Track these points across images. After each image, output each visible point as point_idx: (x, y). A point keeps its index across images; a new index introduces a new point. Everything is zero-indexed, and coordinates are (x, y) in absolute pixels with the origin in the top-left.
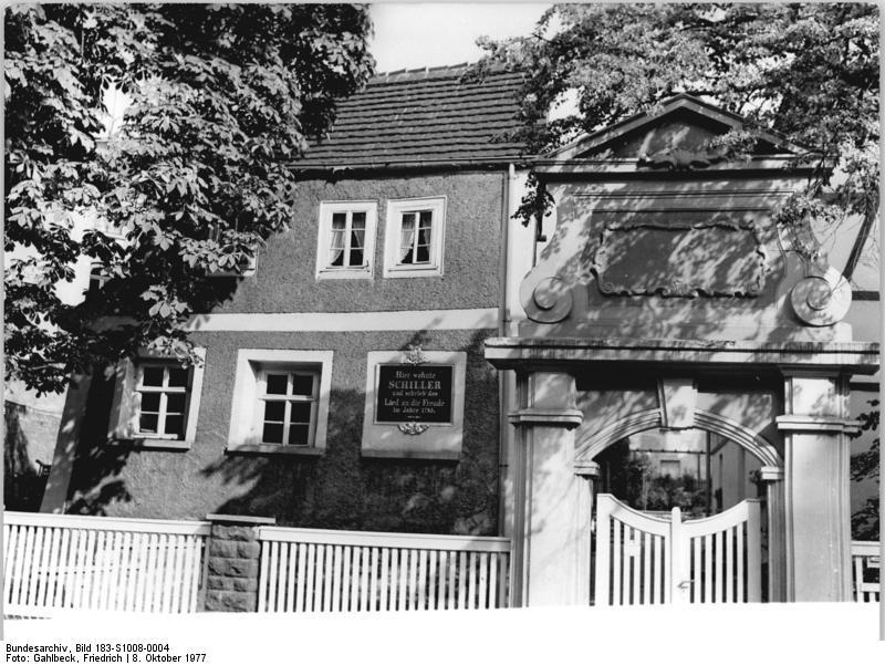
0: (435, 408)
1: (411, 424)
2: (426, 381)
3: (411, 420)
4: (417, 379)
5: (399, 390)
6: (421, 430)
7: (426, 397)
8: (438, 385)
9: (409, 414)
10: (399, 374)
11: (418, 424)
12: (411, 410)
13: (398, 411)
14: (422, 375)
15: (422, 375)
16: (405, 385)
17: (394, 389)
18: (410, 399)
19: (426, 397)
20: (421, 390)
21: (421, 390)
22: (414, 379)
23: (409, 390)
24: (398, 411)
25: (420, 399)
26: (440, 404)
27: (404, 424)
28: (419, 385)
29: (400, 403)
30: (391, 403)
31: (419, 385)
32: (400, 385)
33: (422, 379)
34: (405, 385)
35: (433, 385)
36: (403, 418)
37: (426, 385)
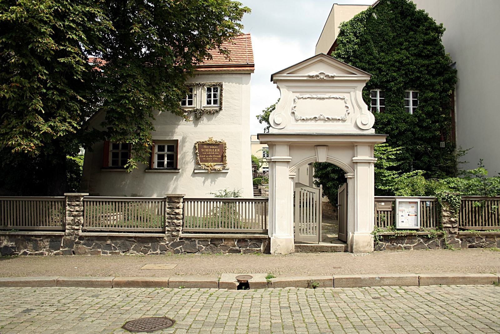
1: (210, 164)
3: (209, 162)
4: (212, 148)
6: (213, 165)
8: (218, 150)
10: (205, 147)
11: (212, 163)
12: (209, 159)
13: (205, 159)
15: (213, 147)
16: (207, 150)
18: (209, 155)
24: (205, 159)
25: (212, 155)
27: (207, 163)
28: (212, 150)
29: (205, 156)
31: (212, 150)
35: (217, 150)
36: (207, 161)
37: (214, 150)
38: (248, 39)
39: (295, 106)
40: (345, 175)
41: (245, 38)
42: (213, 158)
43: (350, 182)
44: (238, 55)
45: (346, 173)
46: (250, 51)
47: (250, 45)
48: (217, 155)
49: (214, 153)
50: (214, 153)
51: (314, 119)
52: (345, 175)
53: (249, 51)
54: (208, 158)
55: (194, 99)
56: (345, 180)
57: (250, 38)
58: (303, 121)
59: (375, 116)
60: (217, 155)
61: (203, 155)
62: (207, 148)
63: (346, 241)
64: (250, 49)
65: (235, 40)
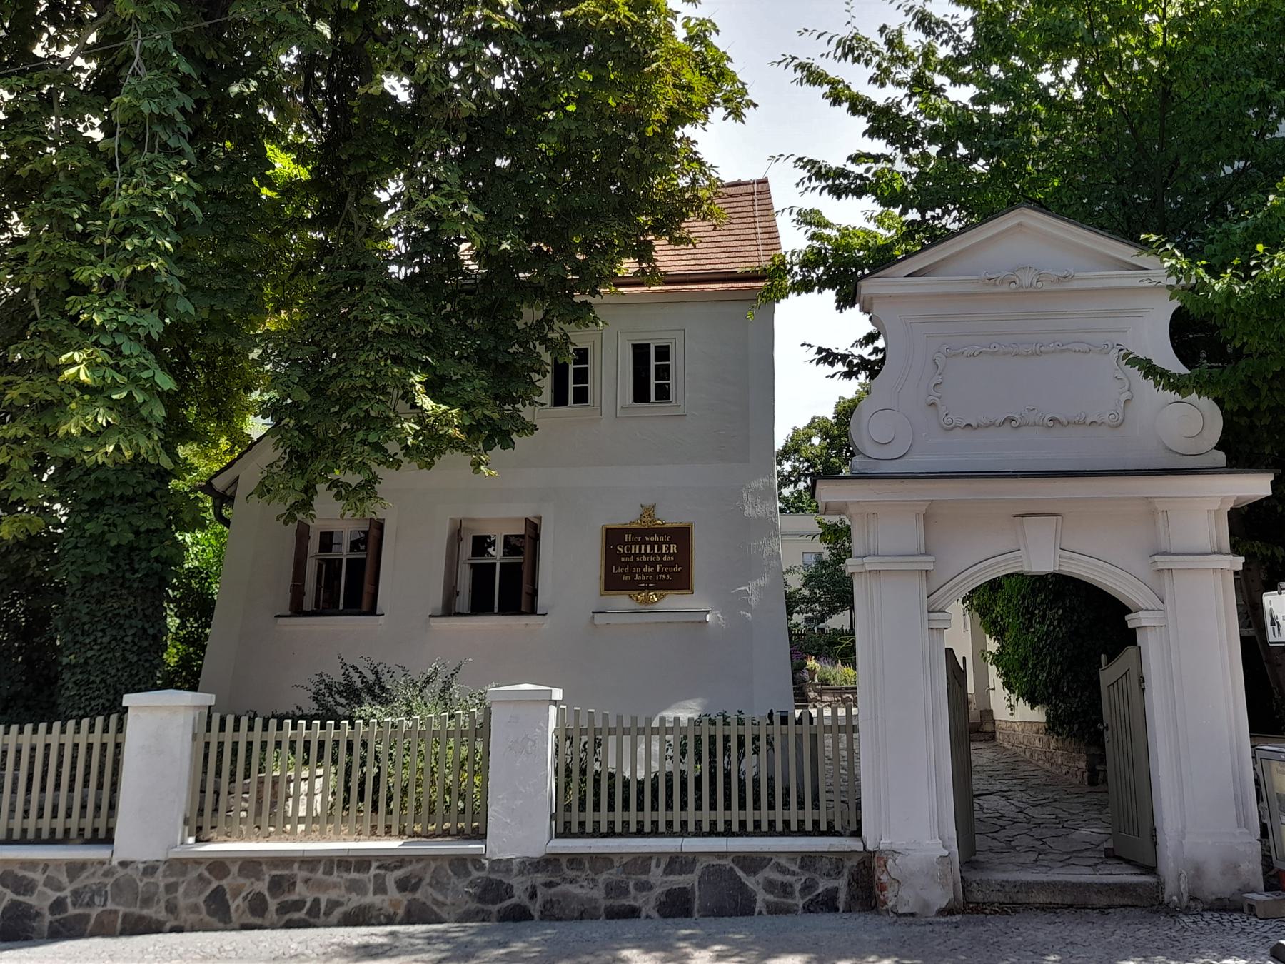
0: (672, 574)
2: (660, 544)
3: (643, 589)
4: (649, 542)
5: (629, 556)
7: (661, 562)
8: (673, 548)
9: (642, 581)
10: (628, 538)
12: (643, 577)
13: (628, 578)
14: (656, 538)
15: (656, 538)
16: (635, 549)
17: (624, 555)
18: (642, 564)
19: (661, 562)
20: (654, 555)
21: (654, 555)
22: (646, 543)
23: (640, 555)
24: (628, 578)
26: (677, 569)
28: (652, 548)
29: (631, 569)
30: (620, 570)
31: (652, 548)
32: (629, 549)
33: (655, 542)
34: (635, 549)
35: (669, 549)
37: (660, 548)
38: (762, 196)
39: (937, 380)
40: (1127, 617)
41: (752, 194)
42: (655, 573)
43: (1149, 644)
44: (731, 244)
45: (1130, 612)
46: (770, 230)
47: (772, 223)
48: (666, 564)
49: (658, 558)
50: (658, 558)
51: (1007, 424)
52: (1127, 617)
53: (767, 230)
54: (640, 574)
55: (592, 386)
56: (1130, 638)
57: (768, 191)
58: (968, 429)
59: (1222, 410)
60: (666, 564)
61: (625, 564)
62: (635, 543)
63: (1149, 863)
64: (767, 224)
65: (720, 201)
